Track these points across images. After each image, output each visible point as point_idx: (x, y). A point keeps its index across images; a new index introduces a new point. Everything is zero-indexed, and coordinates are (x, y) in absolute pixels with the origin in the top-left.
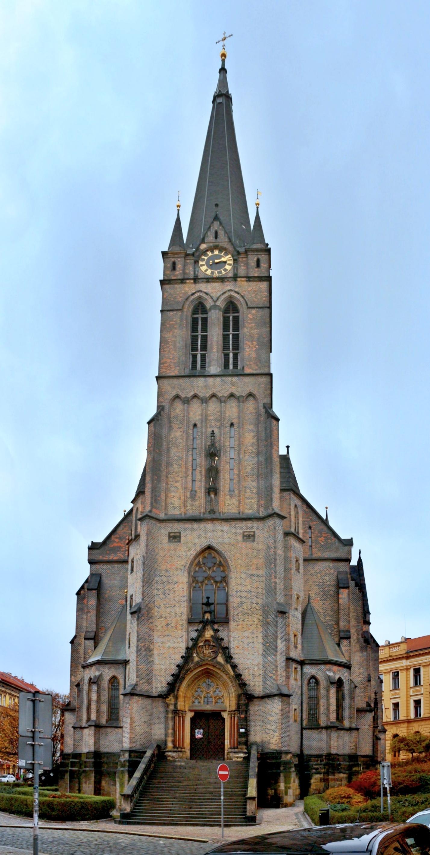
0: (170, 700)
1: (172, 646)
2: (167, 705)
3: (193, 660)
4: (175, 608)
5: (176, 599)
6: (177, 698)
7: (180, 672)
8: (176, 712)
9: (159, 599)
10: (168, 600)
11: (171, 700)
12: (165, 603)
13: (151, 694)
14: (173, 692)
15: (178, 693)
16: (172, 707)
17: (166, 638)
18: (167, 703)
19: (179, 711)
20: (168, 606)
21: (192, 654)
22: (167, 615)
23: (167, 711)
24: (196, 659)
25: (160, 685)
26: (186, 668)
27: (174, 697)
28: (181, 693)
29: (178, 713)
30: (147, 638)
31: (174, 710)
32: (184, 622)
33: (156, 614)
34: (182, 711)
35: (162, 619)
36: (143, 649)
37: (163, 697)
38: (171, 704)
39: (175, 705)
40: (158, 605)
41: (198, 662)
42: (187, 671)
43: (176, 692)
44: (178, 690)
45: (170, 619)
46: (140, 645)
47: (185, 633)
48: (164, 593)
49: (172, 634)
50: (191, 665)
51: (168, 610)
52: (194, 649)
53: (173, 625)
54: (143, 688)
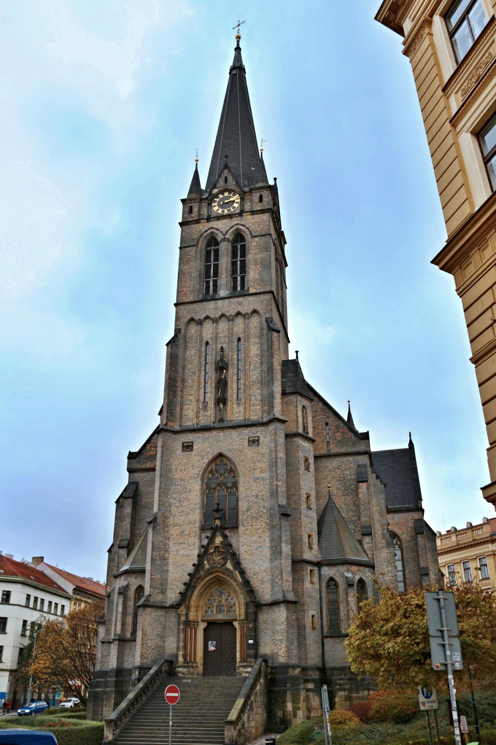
0: (182, 611)
1: (185, 554)
2: (179, 616)
3: (204, 568)
4: (189, 516)
5: (190, 507)
6: (188, 608)
7: (191, 580)
8: (188, 623)
9: (175, 508)
10: (182, 508)
11: (182, 610)
12: (180, 511)
13: (165, 605)
14: (185, 601)
15: (189, 602)
16: (183, 618)
17: (181, 546)
18: (178, 614)
19: (190, 622)
20: (182, 514)
21: (203, 561)
22: (182, 523)
23: (178, 622)
24: (207, 566)
25: (172, 596)
26: (197, 576)
27: (185, 607)
28: (192, 603)
29: (190, 624)
30: (163, 547)
31: (185, 621)
32: (197, 529)
33: (172, 523)
34: (194, 622)
35: (177, 527)
36: (158, 558)
37: (175, 607)
38: (183, 615)
39: (187, 615)
40: (174, 514)
41: (208, 569)
42: (198, 579)
43: (187, 602)
44: (190, 600)
45: (185, 527)
46: (155, 554)
47: (197, 541)
48: (180, 501)
49: (186, 542)
50: (202, 573)
51: (183, 518)
52: (204, 557)
53: (186, 532)
54: (157, 598)
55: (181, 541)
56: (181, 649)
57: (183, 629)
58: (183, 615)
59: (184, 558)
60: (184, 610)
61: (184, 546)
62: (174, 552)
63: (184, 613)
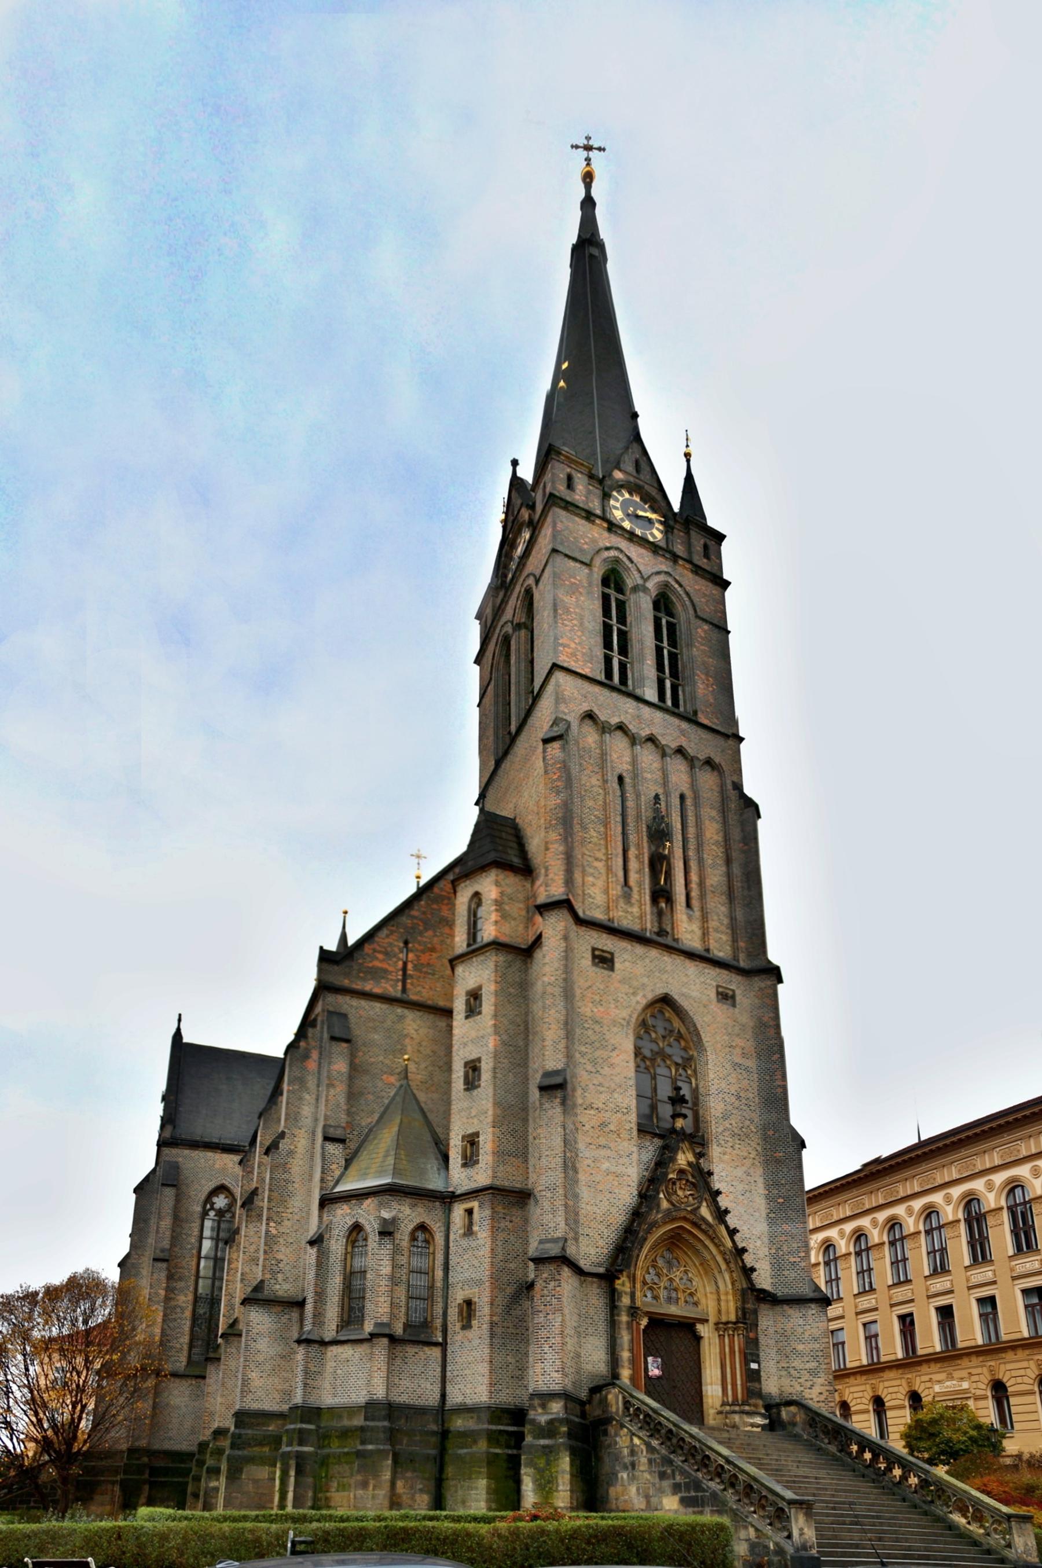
0: (623, 1285)
1: (613, 1169)
14: (628, 1266)
17: (603, 1152)
27: (628, 1277)
31: (631, 1307)
38: (626, 1293)
43: (632, 1269)
45: (608, 1115)
53: (612, 1127)
55: (602, 1141)
56: (626, 1364)
57: (628, 1323)
58: (626, 1293)
59: (610, 1177)
60: (628, 1284)
61: (608, 1152)
62: (589, 1162)
63: (628, 1290)
